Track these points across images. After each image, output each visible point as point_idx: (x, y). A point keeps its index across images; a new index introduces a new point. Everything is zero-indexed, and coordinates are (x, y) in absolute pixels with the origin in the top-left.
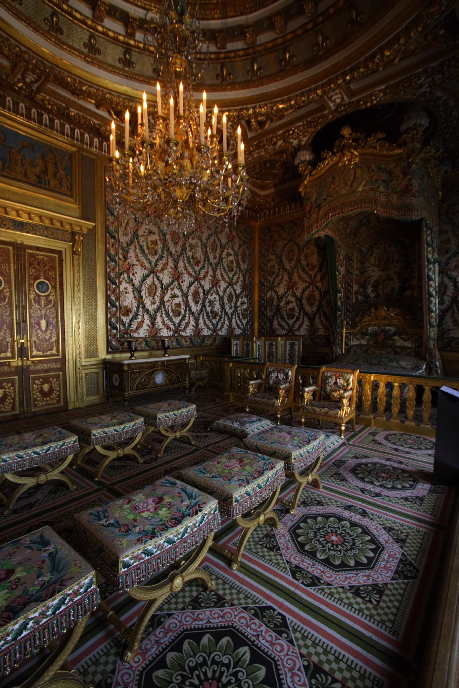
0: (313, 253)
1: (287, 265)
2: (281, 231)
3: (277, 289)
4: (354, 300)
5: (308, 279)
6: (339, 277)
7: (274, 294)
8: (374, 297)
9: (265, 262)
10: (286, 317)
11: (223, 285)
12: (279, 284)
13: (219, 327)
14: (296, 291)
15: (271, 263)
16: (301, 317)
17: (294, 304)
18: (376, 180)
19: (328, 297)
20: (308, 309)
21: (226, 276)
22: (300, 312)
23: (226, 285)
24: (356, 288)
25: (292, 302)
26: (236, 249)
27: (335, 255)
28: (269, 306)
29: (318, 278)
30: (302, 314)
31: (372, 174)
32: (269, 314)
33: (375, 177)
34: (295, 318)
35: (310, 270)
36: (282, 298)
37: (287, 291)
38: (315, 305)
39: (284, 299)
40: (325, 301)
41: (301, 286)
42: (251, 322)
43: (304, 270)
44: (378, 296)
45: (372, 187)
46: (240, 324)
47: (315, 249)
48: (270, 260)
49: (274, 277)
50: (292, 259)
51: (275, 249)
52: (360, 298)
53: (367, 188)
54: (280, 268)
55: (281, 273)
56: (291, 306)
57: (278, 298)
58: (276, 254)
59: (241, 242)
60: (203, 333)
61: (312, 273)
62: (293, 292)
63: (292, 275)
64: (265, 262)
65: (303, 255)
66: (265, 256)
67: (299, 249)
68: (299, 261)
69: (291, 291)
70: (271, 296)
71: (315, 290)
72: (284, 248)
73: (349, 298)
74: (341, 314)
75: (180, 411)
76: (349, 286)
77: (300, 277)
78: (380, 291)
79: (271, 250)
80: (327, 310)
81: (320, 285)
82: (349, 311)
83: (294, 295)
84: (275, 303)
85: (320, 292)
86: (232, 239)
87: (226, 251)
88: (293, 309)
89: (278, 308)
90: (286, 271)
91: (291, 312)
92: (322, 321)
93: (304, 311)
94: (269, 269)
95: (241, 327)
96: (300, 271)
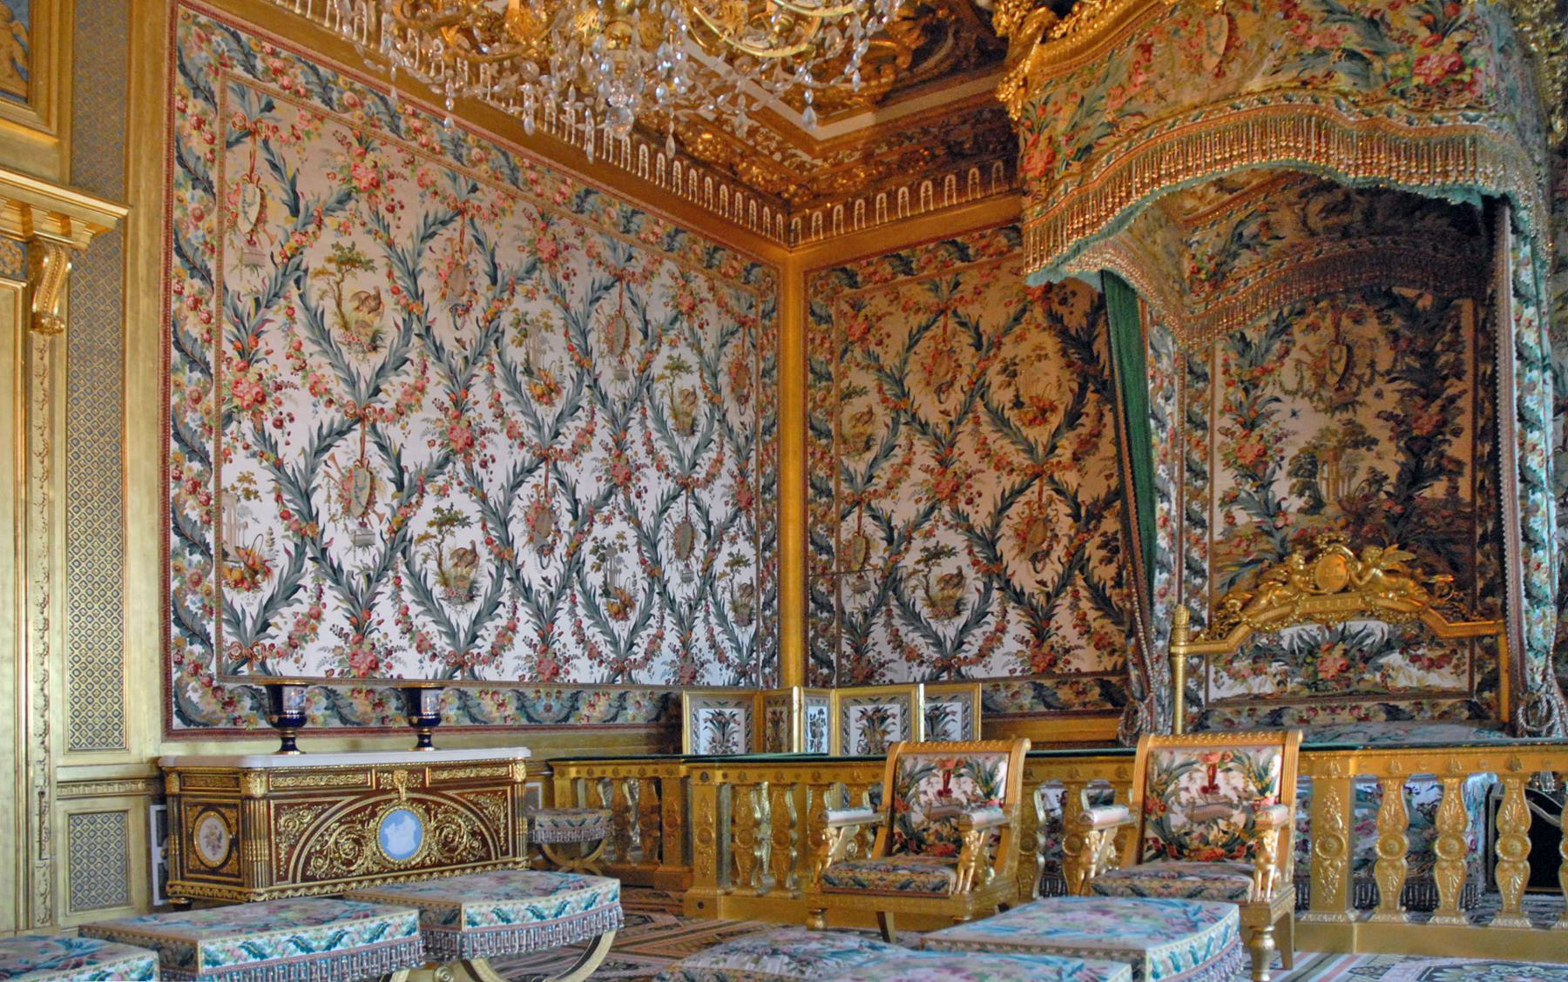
0: (1039, 358)
1: (928, 408)
2: (901, 277)
3: (885, 505)
4: (1219, 526)
5: (1020, 459)
6: (1159, 438)
7: (870, 526)
8: (1300, 510)
9: (832, 399)
10: (925, 613)
11: (655, 485)
12: (890, 487)
13: (639, 652)
14: (968, 509)
15: (857, 405)
16: (995, 607)
17: (963, 560)
18: (1320, 52)
19: (1110, 524)
20: (1023, 576)
21: (666, 452)
22: (988, 588)
23: (669, 485)
24: (1224, 480)
25: (951, 553)
26: (708, 347)
27: (1142, 352)
28: (849, 571)
29: (1065, 451)
30: (996, 594)
31: (1303, 30)
32: (853, 604)
33: (1315, 41)
34: (966, 615)
35: (1032, 422)
36: (909, 539)
37: (932, 509)
38: (1054, 556)
39: (918, 543)
40: (1098, 540)
41: (991, 486)
42: (770, 640)
43: (1000, 421)
44: (1316, 506)
45: (1305, 76)
46: (727, 644)
47: (1050, 343)
48: (848, 395)
49: (869, 456)
50: (951, 384)
51: (878, 350)
52: (1242, 517)
53: (1282, 79)
54: (896, 422)
55: (902, 440)
56: (947, 566)
57: (890, 540)
58: (880, 369)
59: (730, 324)
60: (574, 676)
61: (1039, 435)
62: (956, 512)
63: (952, 445)
64: (832, 399)
65: (996, 366)
66: (829, 377)
67: (978, 346)
68: (979, 388)
69: (946, 509)
70: (859, 532)
71: (1051, 501)
72: (913, 341)
73: (1201, 523)
74: (1169, 582)
75: (555, 901)
76: (1198, 474)
77: (984, 450)
78: (1323, 488)
79: (858, 352)
80: (1106, 573)
81: (1070, 478)
82: (1199, 573)
83: (962, 522)
84: (877, 558)
85: (1076, 506)
86: (692, 308)
87: (665, 350)
88: (958, 579)
89: (891, 581)
90: (924, 433)
91: (949, 592)
92: (1083, 618)
93: (1006, 585)
94: (847, 429)
95: (732, 655)
96: (986, 429)
